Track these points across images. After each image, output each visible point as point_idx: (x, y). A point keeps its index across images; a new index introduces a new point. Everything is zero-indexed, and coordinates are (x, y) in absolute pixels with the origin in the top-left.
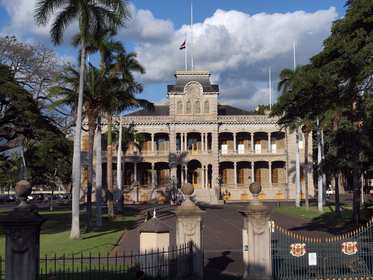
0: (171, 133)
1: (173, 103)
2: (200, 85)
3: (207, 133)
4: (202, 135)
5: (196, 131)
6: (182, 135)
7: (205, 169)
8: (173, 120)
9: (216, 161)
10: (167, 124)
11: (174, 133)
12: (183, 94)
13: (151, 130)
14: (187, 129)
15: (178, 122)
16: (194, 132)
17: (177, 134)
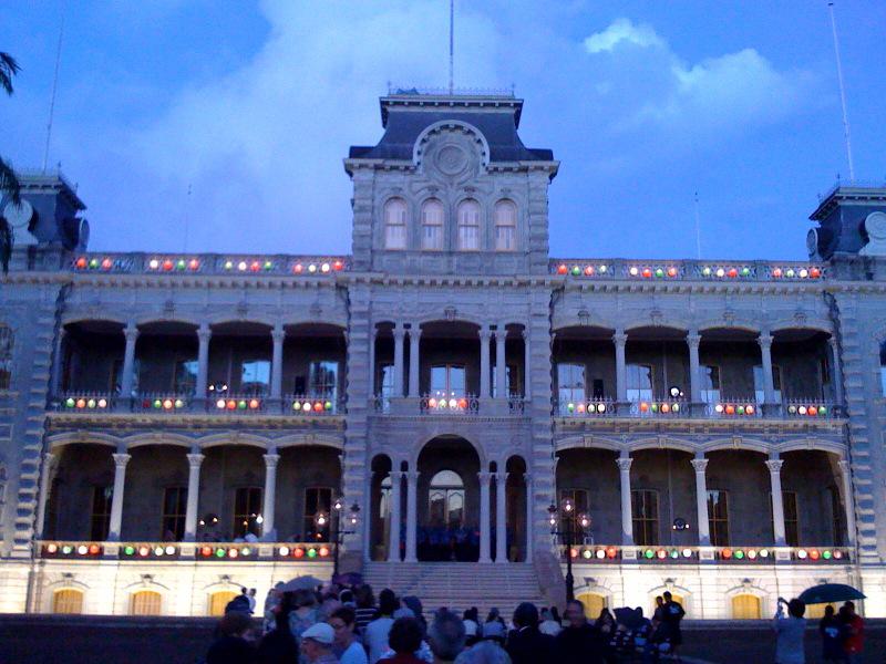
0: (355, 322)
1: (368, 202)
2: (479, 135)
3: (503, 327)
4: (485, 333)
5: (459, 318)
6: (399, 331)
7: (494, 476)
9: (544, 442)
10: (337, 285)
11: (365, 322)
12: (407, 168)
14: (421, 308)
15: (381, 276)
16: (450, 318)
17: (378, 325)
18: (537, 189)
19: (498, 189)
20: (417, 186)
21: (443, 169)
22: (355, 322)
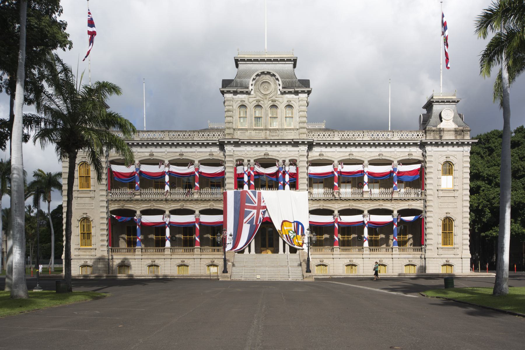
8: (231, 137)
12: (247, 92)
13: (194, 154)
15: (238, 140)
18: (302, 100)
19: (285, 100)
20: (251, 100)
21: (262, 92)
22: (227, 159)
